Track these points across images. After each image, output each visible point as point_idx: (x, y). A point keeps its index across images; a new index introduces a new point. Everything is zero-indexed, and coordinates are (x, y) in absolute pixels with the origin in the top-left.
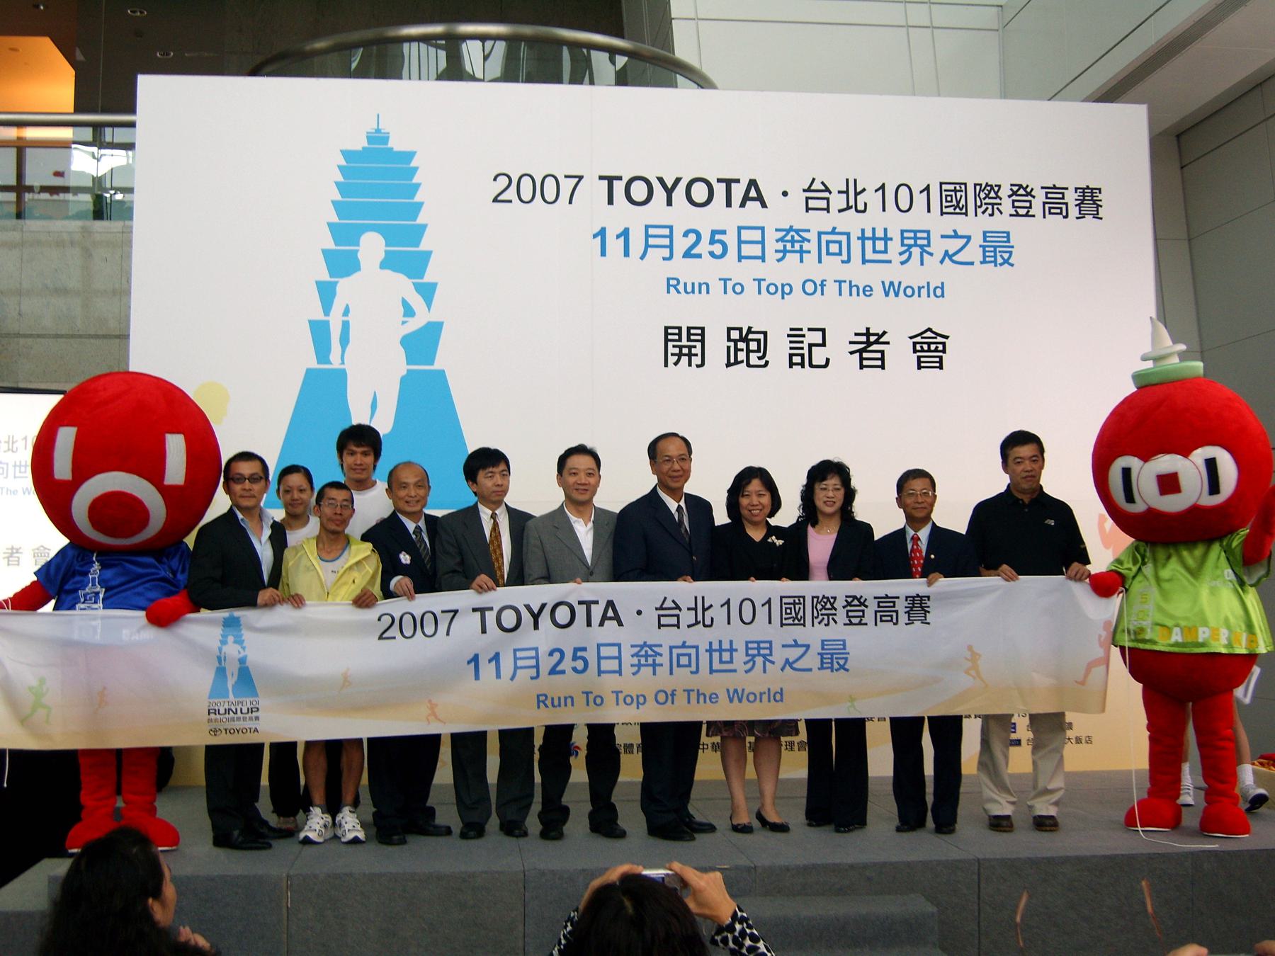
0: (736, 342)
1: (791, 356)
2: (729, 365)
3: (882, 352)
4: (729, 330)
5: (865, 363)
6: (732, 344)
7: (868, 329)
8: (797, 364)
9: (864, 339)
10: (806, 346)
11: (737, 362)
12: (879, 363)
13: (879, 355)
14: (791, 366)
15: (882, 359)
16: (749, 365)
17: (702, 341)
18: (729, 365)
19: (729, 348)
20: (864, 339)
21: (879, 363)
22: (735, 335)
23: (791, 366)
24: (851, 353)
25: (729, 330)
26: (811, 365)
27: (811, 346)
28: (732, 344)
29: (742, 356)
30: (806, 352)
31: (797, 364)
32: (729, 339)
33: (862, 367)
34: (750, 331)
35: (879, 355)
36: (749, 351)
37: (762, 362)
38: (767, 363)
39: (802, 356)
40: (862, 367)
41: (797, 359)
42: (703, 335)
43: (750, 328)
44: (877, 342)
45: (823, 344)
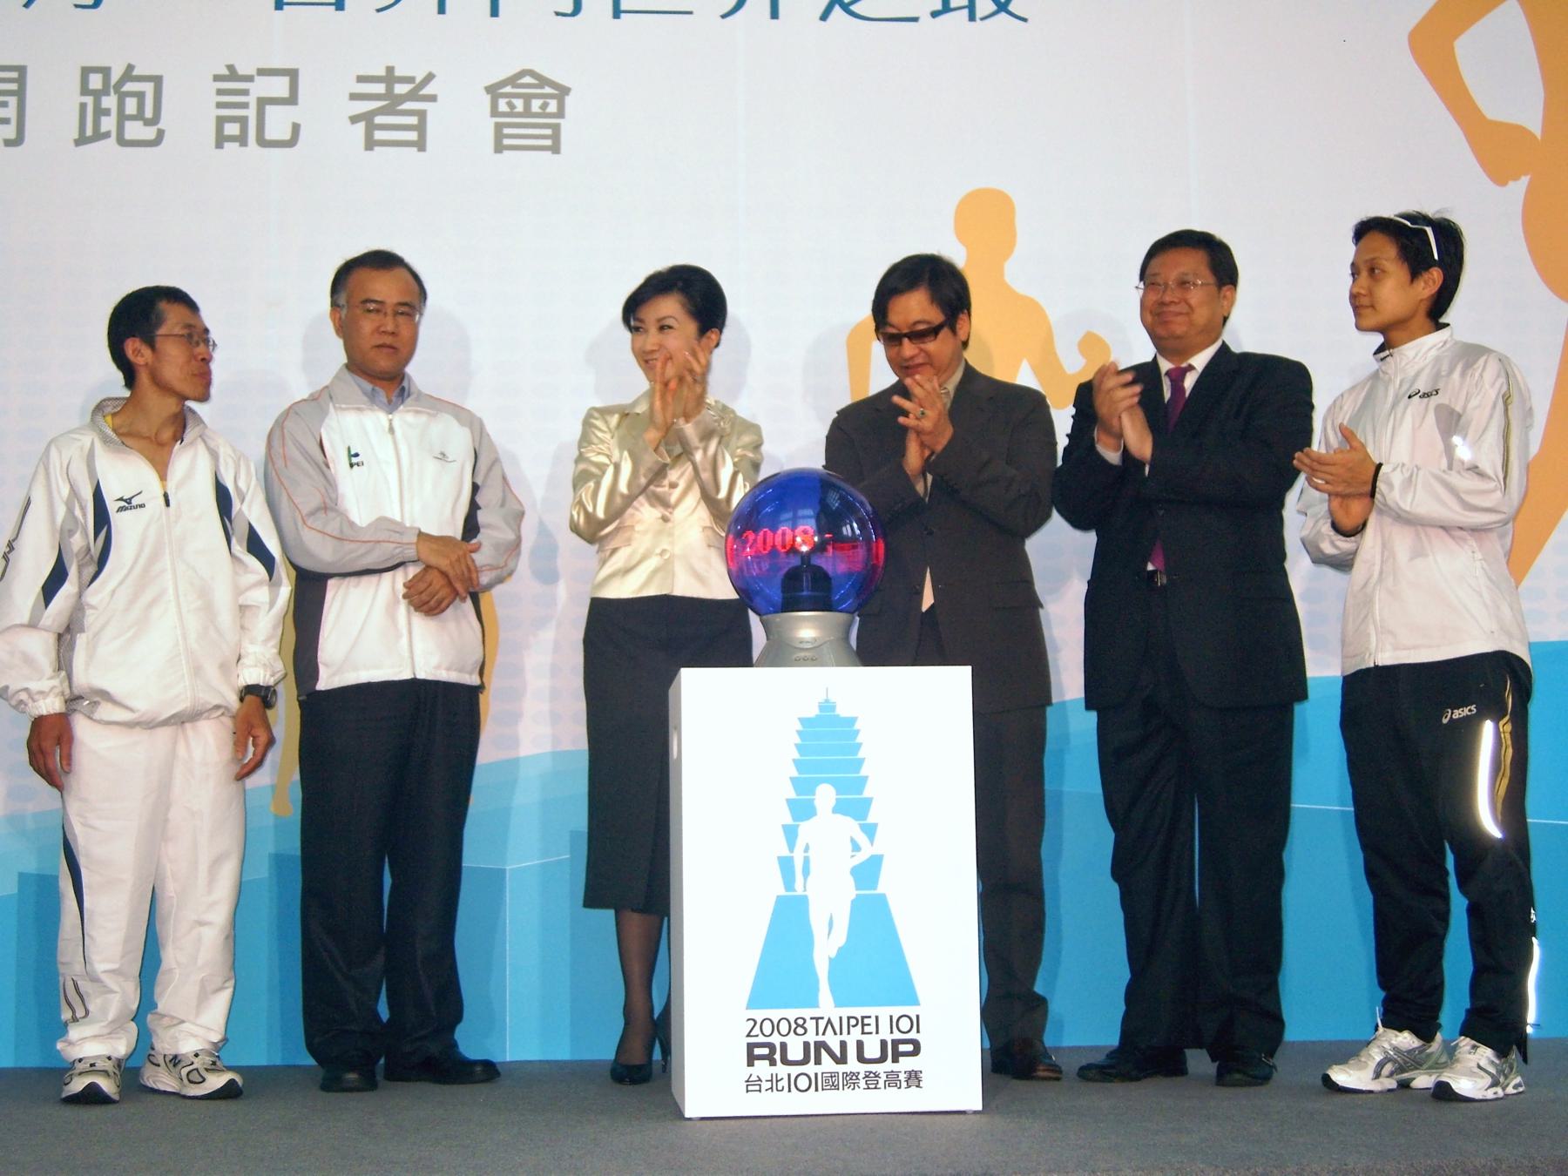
0: (97, 95)
1: (221, 121)
2: (81, 141)
3: (422, 115)
4: (86, 72)
5: (379, 135)
6: (89, 100)
7: (390, 70)
8: (232, 139)
9: (380, 88)
10: (252, 100)
11: (99, 136)
12: (413, 136)
13: (413, 120)
14: (219, 145)
15: (421, 128)
16: (122, 142)
17: (21, 94)
18: (81, 141)
19: (83, 107)
20: (380, 88)
21: (413, 136)
22: (96, 82)
23: (219, 145)
24: (354, 119)
25: (86, 72)
26: (263, 142)
27: (263, 103)
28: (89, 100)
29: (108, 124)
30: (251, 113)
31: (232, 139)
32: (85, 90)
33: (370, 144)
34: (129, 75)
35: (413, 120)
36: (122, 118)
37: (149, 133)
38: (161, 133)
39: (243, 121)
40: (370, 144)
41: (232, 129)
42: (21, 80)
43: (130, 67)
44: (413, 96)
45: (292, 99)
